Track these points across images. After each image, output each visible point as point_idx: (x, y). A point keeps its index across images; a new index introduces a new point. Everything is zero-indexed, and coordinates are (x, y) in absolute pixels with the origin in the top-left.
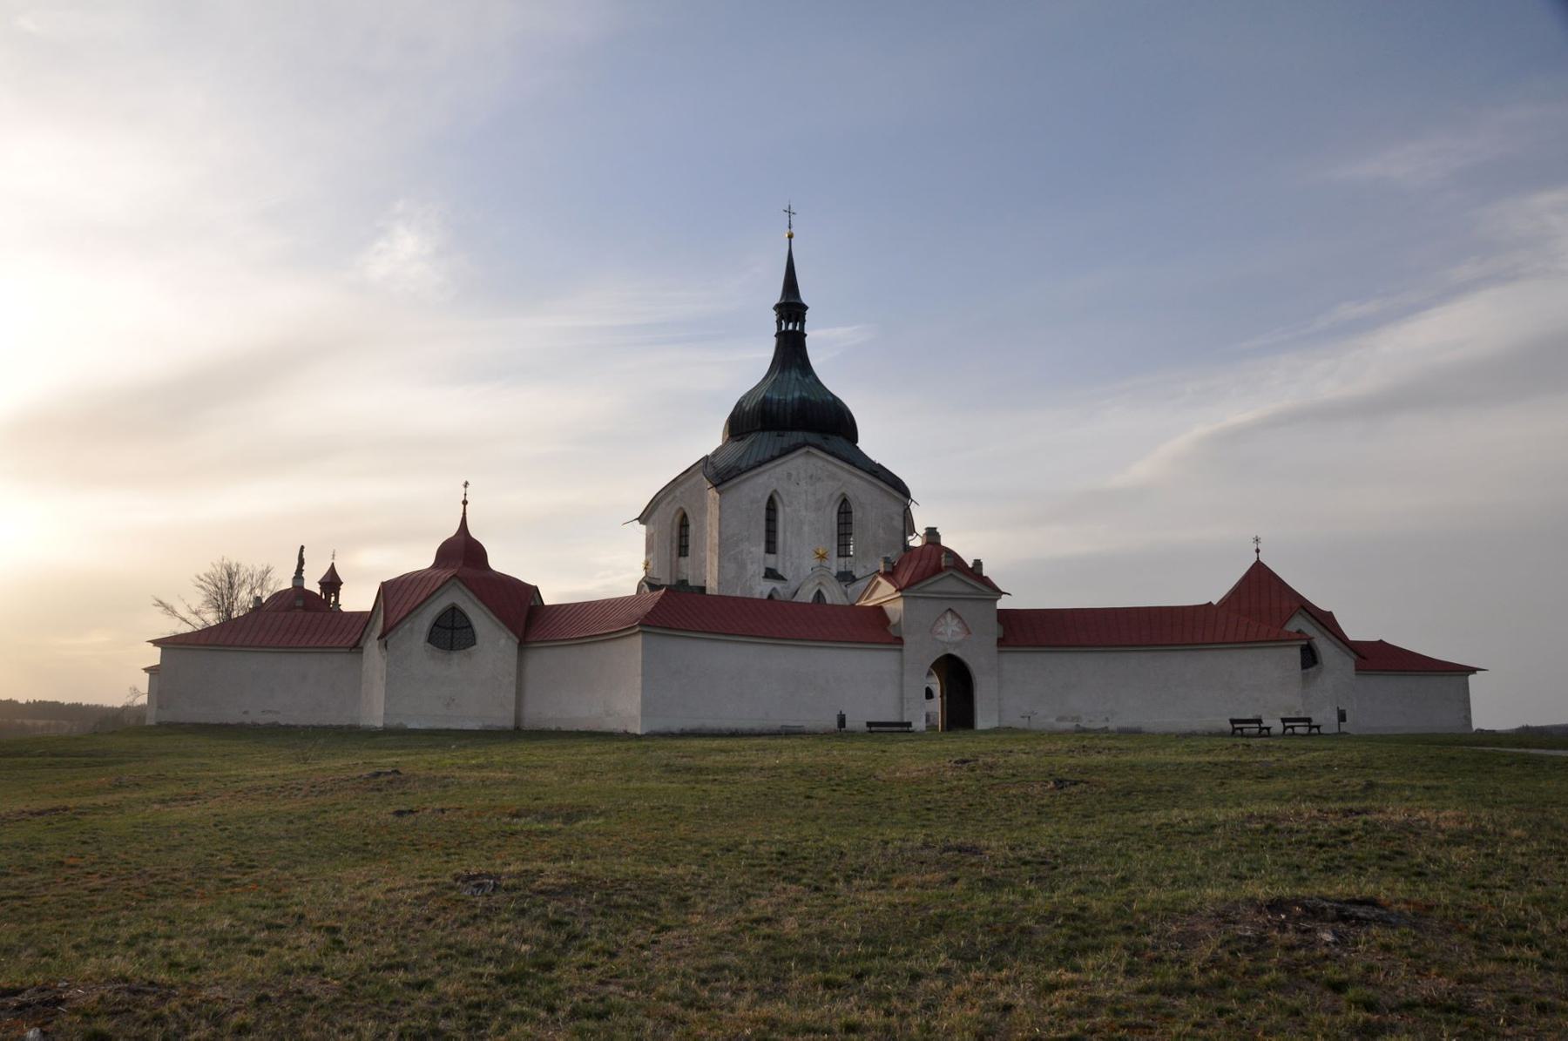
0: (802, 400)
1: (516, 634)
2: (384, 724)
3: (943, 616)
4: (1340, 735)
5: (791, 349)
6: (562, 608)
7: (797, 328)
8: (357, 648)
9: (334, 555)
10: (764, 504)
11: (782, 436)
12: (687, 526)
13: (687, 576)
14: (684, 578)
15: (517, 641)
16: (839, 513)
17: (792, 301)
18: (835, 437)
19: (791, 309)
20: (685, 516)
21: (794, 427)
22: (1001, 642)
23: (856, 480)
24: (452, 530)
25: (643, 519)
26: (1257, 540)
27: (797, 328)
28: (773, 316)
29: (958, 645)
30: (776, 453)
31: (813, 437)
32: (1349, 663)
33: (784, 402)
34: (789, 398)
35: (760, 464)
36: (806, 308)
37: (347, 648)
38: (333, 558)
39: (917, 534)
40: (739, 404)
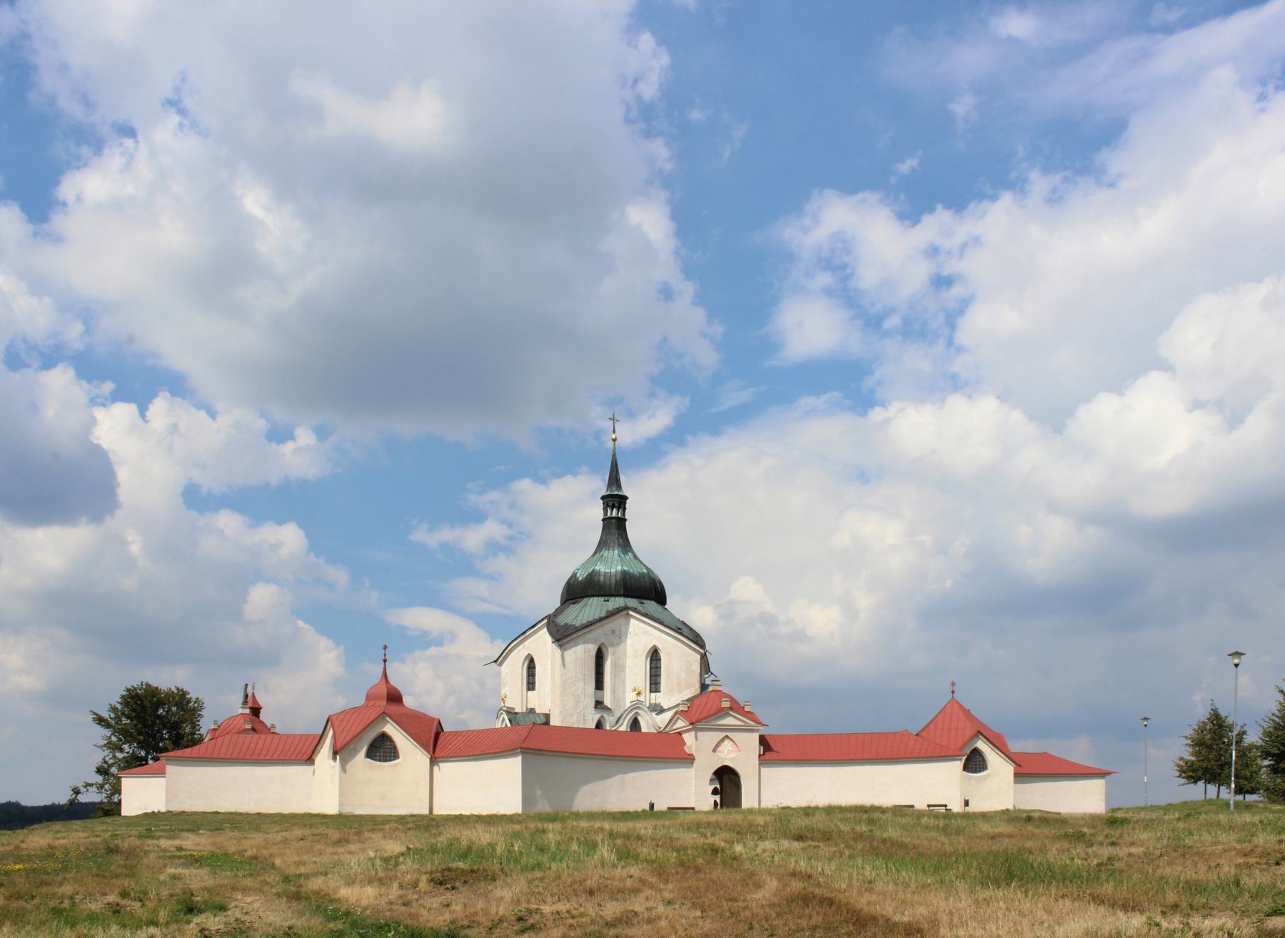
0: (624, 573)
1: (428, 751)
2: (340, 811)
3: (722, 740)
4: (966, 816)
6: (458, 734)
7: (620, 515)
8: (310, 760)
9: (253, 687)
11: (608, 601)
12: (534, 667)
13: (534, 705)
14: (532, 707)
15: (430, 756)
16: (651, 660)
17: (616, 493)
18: (649, 602)
26: (953, 684)
27: (620, 515)
29: (732, 759)
30: (603, 615)
31: (632, 602)
32: (1008, 769)
33: (609, 575)
34: (613, 570)
37: (302, 760)
38: (253, 689)
39: (712, 673)
40: (574, 575)
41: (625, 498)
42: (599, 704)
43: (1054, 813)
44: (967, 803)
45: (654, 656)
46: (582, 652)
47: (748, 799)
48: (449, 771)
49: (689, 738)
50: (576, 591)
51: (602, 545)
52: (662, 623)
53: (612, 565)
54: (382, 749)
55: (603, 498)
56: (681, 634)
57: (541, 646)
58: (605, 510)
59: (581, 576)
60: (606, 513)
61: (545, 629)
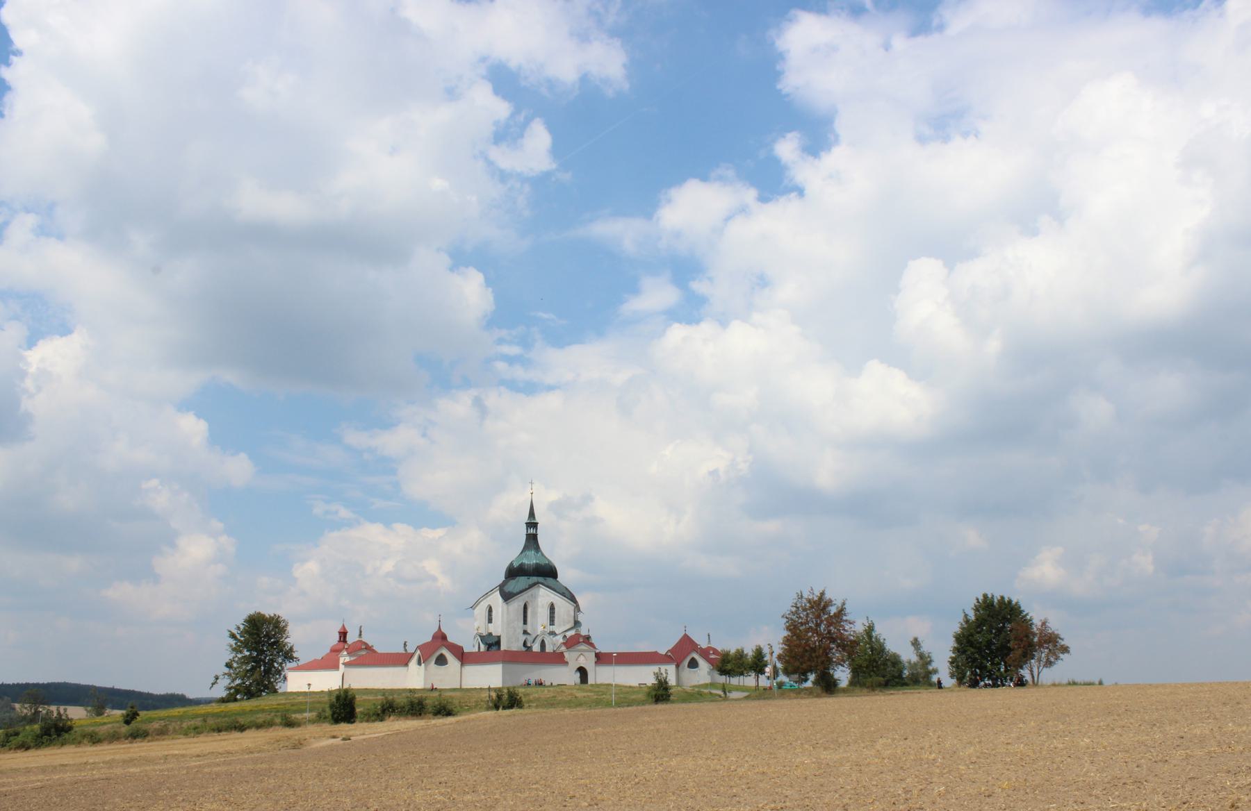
0: (537, 564)
3: (580, 655)
5: (532, 541)
8: (406, 665)
19: (532, 525)
21: (534, 575)
22: (596, 662)
24: (436, 629)
28: (525, 526)
30: (527, 587)
31: (541, 579)
36: (538, 523)
40: (511, 564)
41: (538, 523)
42: (525, 632)
43: (626, 687)
45: (552, 608)
46: (517, 604)
47: (591, 680)
49: (566, 655)
50: (514, 572)
51: (526, 548)
52: (555, 591)
53: (531, 560)
54: (441, 661)
55: (526, 523)
56: (565, 596)
57: (496, 599)
59: (516, 565)
60: (527, 531)
61: (498, 592)
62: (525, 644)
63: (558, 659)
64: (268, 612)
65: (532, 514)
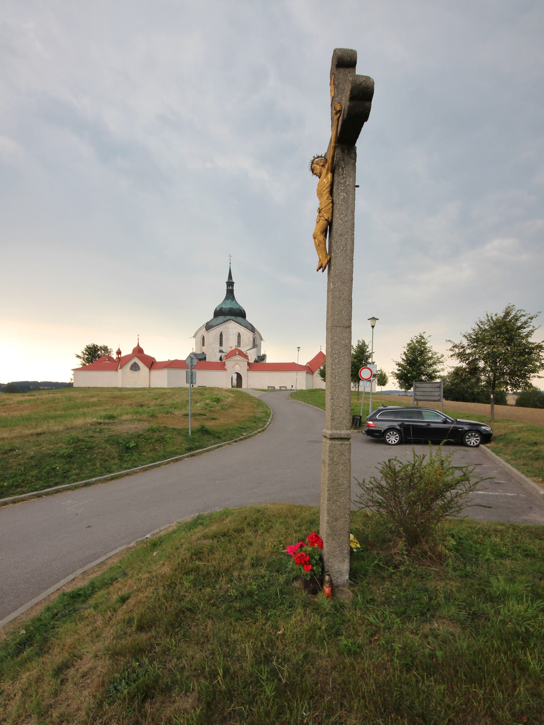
0: (231, 308)
1: (148, 367)
5: (230, 293)
10: (219, 335)
19: (230, 284)
20: (204, 336)
21: (228, 315)
22: (248, 370)
23: (242, 329)
24: (136, 345)
25: (194, 337)
35: (218, 325)
40: (216, 309)
44: (292, 386)
45: (239, 336)
48: (155, 373)
50: (218, 313)
51: (227, 298)
52: (241, 325)
53: (229, 305)
56: (247, 328)
58: (227, 288)
62: (221, 359)
63: (220, 366)
64: (100, 343)
65: (230, 277)
